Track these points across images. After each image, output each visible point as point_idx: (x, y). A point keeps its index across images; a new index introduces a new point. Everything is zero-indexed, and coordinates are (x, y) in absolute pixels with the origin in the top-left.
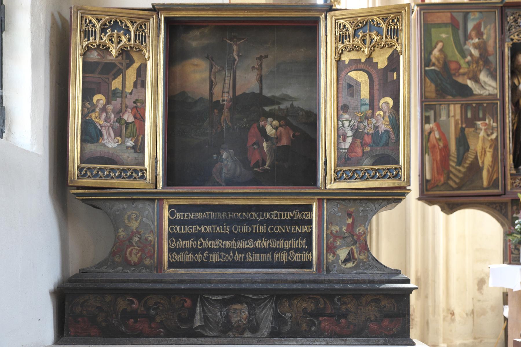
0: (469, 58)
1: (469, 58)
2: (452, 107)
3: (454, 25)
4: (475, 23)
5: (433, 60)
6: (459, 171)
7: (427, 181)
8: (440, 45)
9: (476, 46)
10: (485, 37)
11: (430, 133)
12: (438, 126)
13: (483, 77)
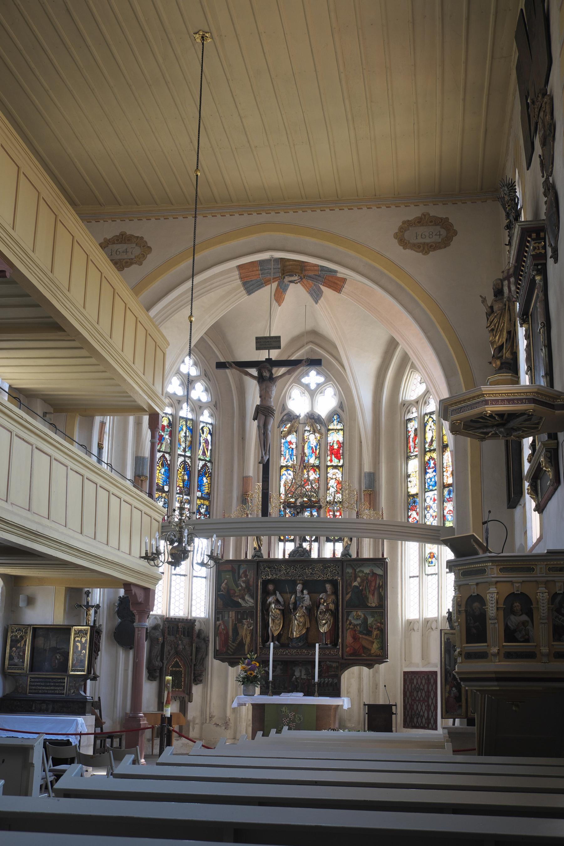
0: (240, 588)
1: (240, 588)
2: (231, 613)
3: (233, 571)
4: (244, 570)
5: (222, 589)
6: (233, 646)
7: (217, 650)
8: (226, 581)
9: (244, 582)
10: (248, 577)
11: (219, 626)
12: (224, 622)
13: (247, 597)
